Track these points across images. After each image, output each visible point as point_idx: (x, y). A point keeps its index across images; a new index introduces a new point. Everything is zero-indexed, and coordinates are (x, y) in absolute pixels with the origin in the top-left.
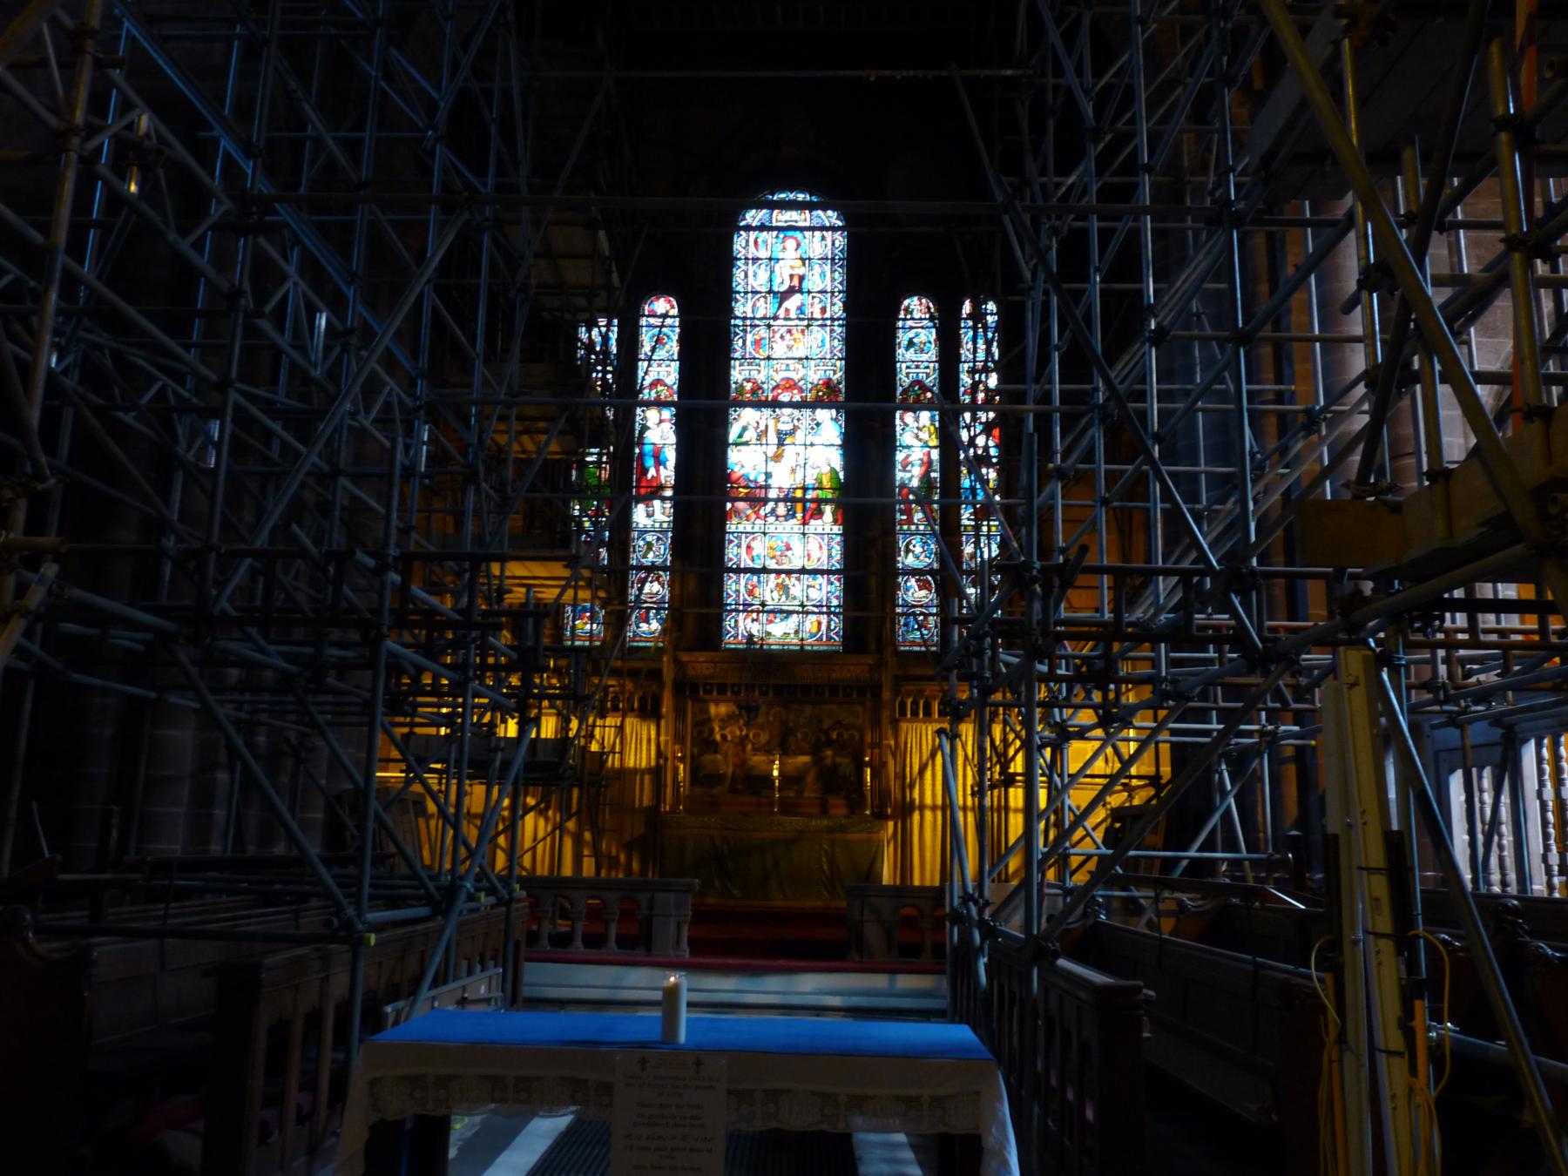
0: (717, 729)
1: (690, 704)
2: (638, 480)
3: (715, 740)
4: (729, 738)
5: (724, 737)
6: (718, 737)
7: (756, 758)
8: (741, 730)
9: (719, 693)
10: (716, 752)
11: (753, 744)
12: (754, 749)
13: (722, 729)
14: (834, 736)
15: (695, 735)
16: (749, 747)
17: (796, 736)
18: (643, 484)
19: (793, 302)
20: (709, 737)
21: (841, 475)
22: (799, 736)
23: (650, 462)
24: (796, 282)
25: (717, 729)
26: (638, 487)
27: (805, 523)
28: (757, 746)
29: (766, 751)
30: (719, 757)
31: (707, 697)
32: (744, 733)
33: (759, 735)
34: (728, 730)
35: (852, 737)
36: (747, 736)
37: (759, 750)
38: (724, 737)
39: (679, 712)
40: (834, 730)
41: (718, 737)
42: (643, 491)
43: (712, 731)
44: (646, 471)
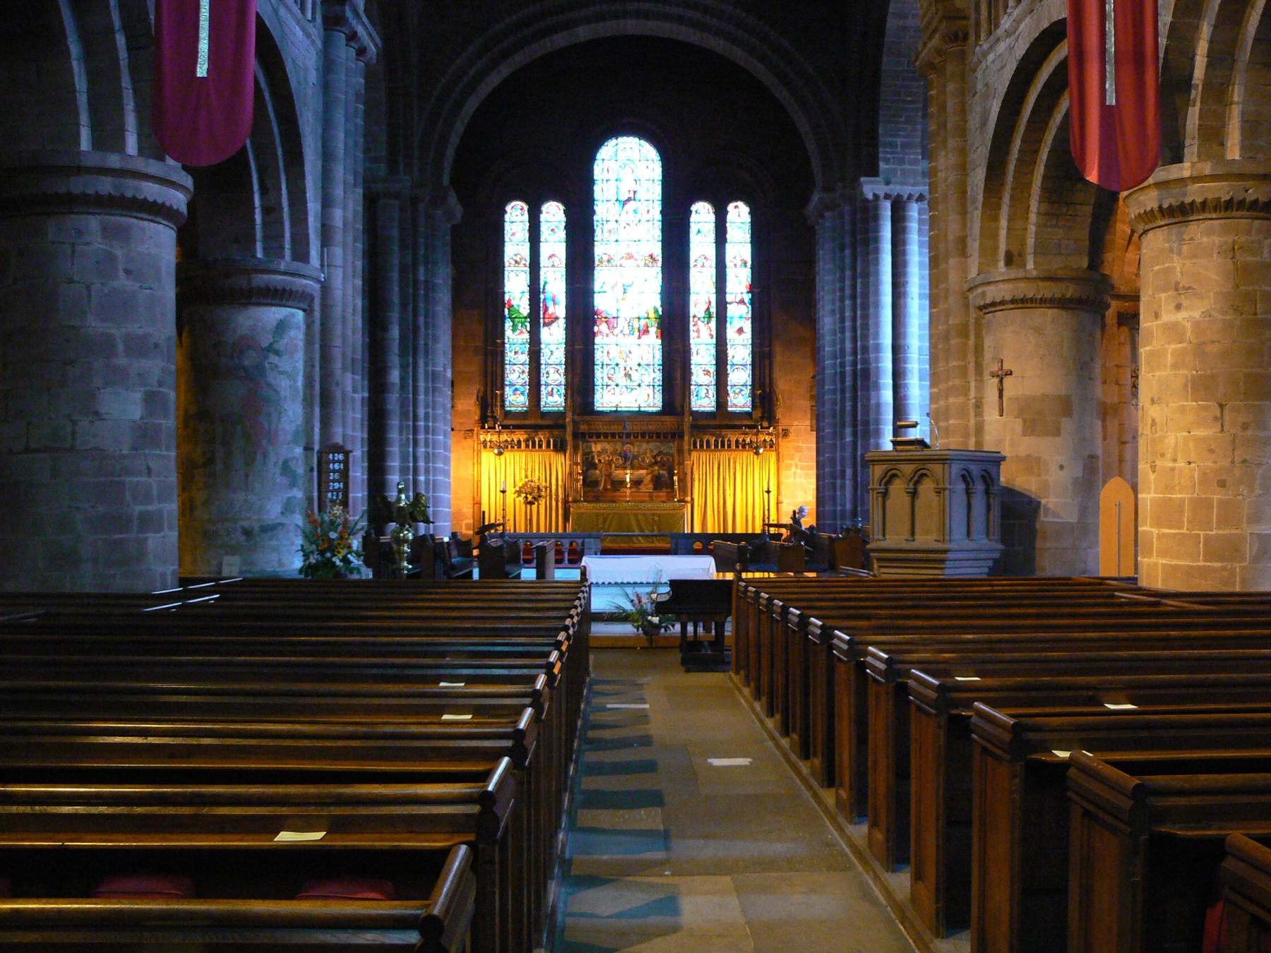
1: (581, 443)
2: (544, 313)
5: (599, 460)
12: (616, 467)
14: (659, 459)
18: (547, 316)
19: (631, 205)
21: (660, 310)
23: (550, 304)
24: (631, 195)
26: (544, 318)
27: (639, 338)
30: (597, 471)
35: (668, 459)
38: (599, 460)
39: (575, 448)
41: (597, 461)
42: (547, 320)
43: (593, 457)
44: (546, 309)
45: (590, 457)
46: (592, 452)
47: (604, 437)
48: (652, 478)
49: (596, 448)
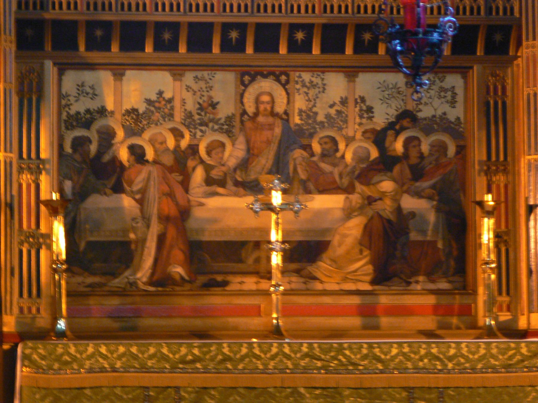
0: (120, 134)
3: (115, 161)
4: (150, 155)
6: (124, 155)
7: (214, 202)
8: (178, 134)
9: (123, 48)
10: (118, 189)
11: (208, 168)
12: (209, 181)
13: (130, 132)
14: (399, 146)
15: (68, 149)
16: (199, 175)
17: (307, 148)
20: (100, 154)
22: (317, 148)
25: (120, 134)
28: (215, 174)
29: (237, 184)
31: (96, 56)
32: (184, 143)
33: (223, 145)
34: (147, 135)
36: (193, 149)
37: (222, 183)
40: (397, 133)
41: (124, 155)
45: (93, 134)
46: (102, 111)
47: (159, 46)
48: (367, 230)
49: (119, 95)
